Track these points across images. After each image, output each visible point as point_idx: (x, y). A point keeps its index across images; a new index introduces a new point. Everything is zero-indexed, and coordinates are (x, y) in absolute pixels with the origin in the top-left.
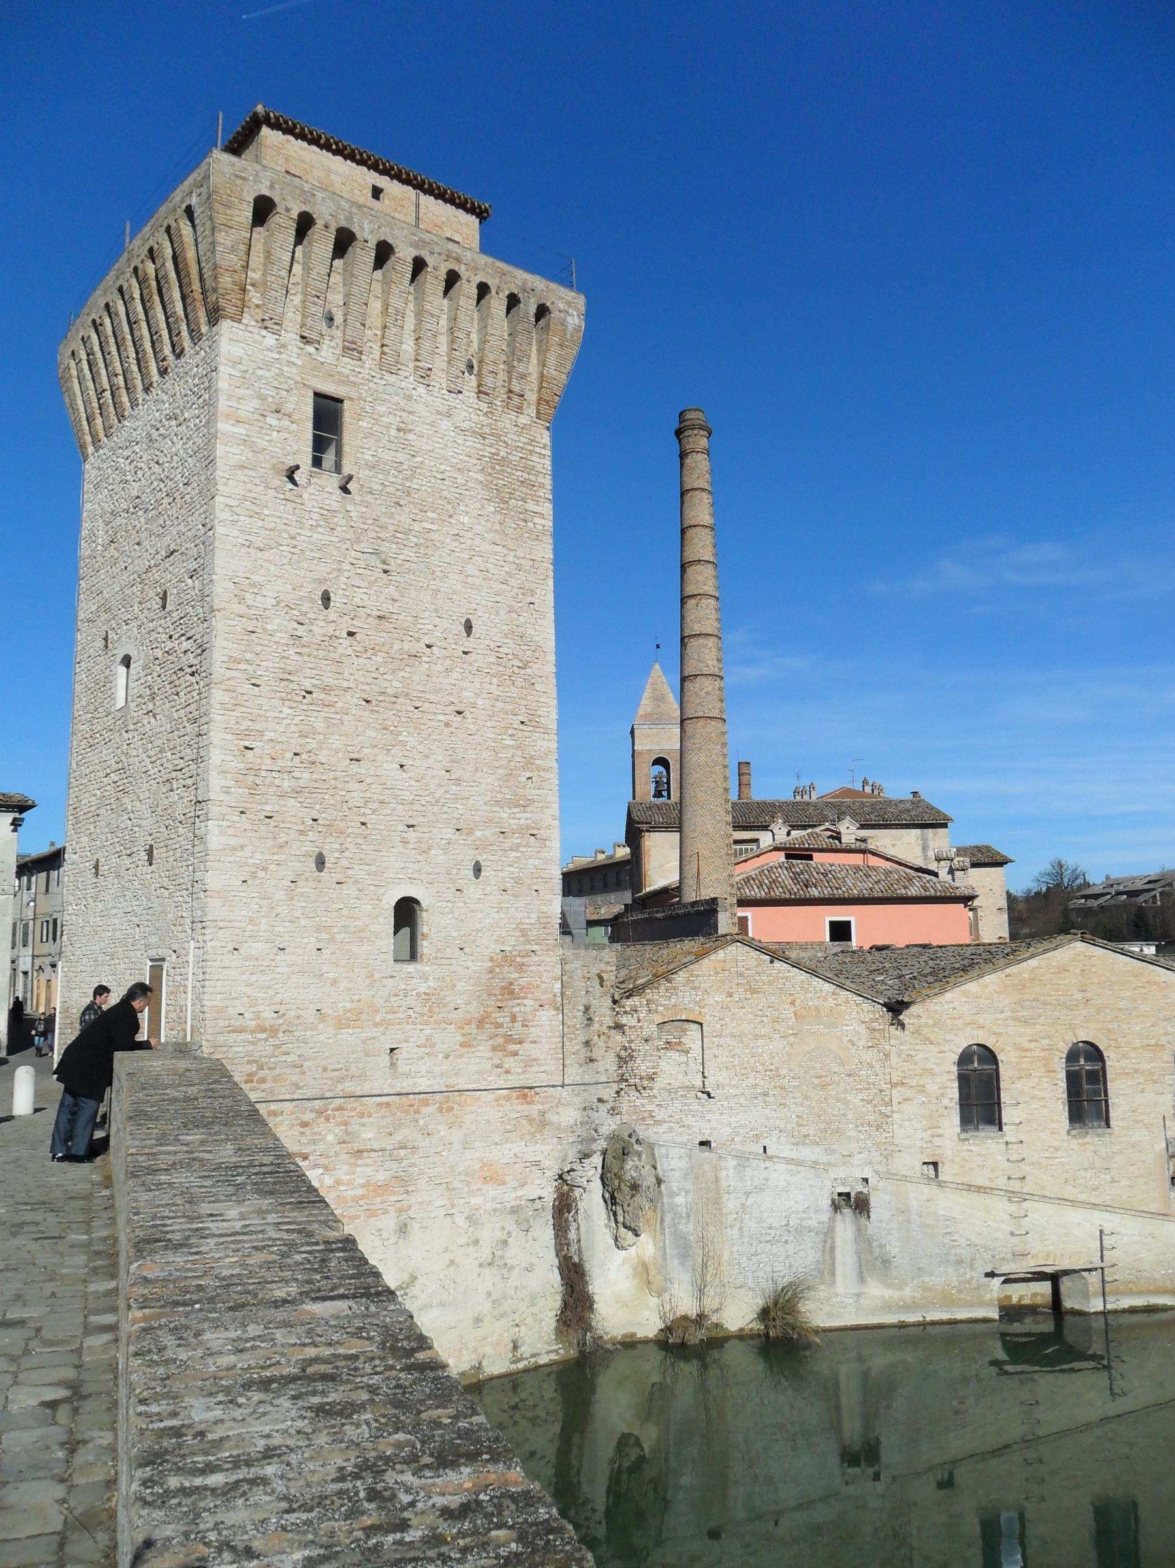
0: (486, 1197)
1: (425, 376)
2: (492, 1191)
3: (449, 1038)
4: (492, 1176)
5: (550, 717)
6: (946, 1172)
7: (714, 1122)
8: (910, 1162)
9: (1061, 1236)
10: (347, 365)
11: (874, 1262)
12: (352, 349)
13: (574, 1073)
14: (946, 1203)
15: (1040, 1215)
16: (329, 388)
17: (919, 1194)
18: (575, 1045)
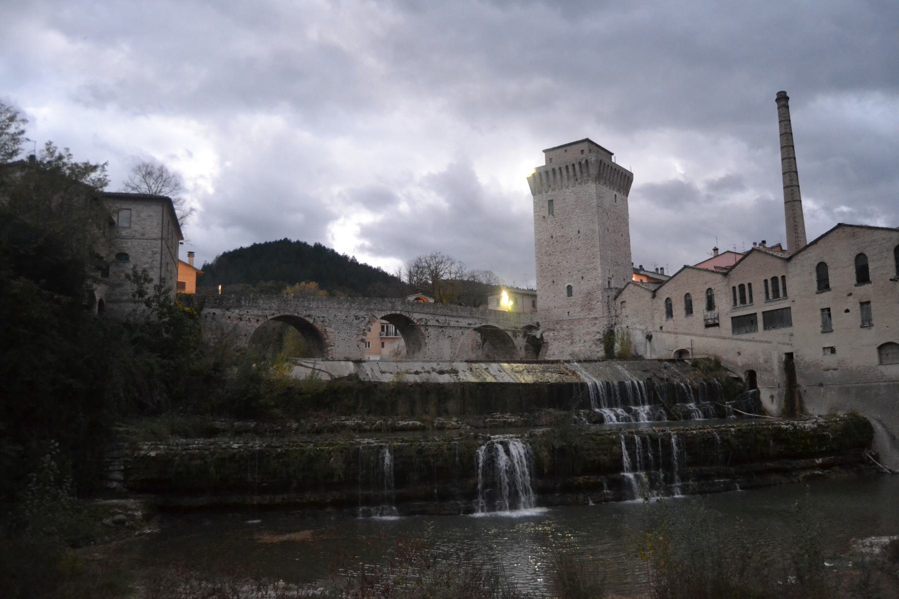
0: (587, 338)
1: (567, 187)
2: (588, 337)
3: (578, 309)
4: (588, 333)
5: (598, 244)
6: (664, 329)
7: (628, 322)
8: (657, 328)
9: (684, 343)
10: (553, 193)
11: (653, 350)
12: (554, 190)
13: (606, 314)
14: (665, 336)
15: (680, 337)
16: (550, 199)
17: (659, 335)
18: (606, 308)
